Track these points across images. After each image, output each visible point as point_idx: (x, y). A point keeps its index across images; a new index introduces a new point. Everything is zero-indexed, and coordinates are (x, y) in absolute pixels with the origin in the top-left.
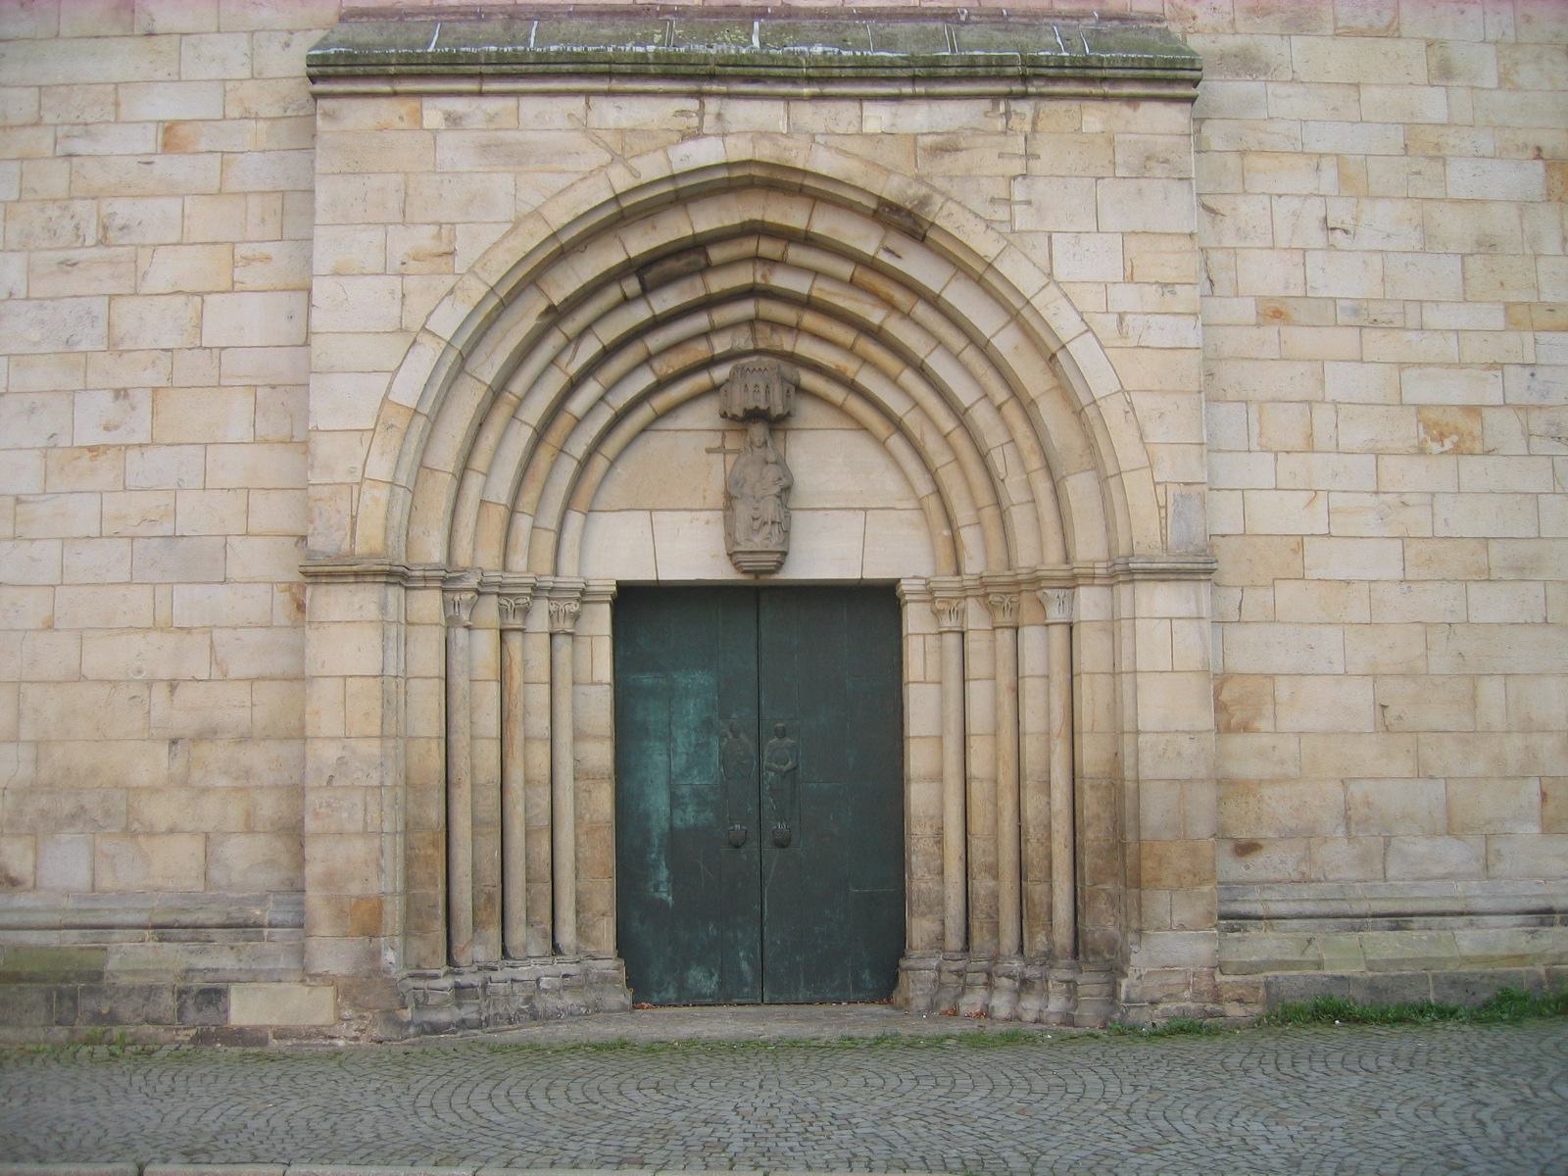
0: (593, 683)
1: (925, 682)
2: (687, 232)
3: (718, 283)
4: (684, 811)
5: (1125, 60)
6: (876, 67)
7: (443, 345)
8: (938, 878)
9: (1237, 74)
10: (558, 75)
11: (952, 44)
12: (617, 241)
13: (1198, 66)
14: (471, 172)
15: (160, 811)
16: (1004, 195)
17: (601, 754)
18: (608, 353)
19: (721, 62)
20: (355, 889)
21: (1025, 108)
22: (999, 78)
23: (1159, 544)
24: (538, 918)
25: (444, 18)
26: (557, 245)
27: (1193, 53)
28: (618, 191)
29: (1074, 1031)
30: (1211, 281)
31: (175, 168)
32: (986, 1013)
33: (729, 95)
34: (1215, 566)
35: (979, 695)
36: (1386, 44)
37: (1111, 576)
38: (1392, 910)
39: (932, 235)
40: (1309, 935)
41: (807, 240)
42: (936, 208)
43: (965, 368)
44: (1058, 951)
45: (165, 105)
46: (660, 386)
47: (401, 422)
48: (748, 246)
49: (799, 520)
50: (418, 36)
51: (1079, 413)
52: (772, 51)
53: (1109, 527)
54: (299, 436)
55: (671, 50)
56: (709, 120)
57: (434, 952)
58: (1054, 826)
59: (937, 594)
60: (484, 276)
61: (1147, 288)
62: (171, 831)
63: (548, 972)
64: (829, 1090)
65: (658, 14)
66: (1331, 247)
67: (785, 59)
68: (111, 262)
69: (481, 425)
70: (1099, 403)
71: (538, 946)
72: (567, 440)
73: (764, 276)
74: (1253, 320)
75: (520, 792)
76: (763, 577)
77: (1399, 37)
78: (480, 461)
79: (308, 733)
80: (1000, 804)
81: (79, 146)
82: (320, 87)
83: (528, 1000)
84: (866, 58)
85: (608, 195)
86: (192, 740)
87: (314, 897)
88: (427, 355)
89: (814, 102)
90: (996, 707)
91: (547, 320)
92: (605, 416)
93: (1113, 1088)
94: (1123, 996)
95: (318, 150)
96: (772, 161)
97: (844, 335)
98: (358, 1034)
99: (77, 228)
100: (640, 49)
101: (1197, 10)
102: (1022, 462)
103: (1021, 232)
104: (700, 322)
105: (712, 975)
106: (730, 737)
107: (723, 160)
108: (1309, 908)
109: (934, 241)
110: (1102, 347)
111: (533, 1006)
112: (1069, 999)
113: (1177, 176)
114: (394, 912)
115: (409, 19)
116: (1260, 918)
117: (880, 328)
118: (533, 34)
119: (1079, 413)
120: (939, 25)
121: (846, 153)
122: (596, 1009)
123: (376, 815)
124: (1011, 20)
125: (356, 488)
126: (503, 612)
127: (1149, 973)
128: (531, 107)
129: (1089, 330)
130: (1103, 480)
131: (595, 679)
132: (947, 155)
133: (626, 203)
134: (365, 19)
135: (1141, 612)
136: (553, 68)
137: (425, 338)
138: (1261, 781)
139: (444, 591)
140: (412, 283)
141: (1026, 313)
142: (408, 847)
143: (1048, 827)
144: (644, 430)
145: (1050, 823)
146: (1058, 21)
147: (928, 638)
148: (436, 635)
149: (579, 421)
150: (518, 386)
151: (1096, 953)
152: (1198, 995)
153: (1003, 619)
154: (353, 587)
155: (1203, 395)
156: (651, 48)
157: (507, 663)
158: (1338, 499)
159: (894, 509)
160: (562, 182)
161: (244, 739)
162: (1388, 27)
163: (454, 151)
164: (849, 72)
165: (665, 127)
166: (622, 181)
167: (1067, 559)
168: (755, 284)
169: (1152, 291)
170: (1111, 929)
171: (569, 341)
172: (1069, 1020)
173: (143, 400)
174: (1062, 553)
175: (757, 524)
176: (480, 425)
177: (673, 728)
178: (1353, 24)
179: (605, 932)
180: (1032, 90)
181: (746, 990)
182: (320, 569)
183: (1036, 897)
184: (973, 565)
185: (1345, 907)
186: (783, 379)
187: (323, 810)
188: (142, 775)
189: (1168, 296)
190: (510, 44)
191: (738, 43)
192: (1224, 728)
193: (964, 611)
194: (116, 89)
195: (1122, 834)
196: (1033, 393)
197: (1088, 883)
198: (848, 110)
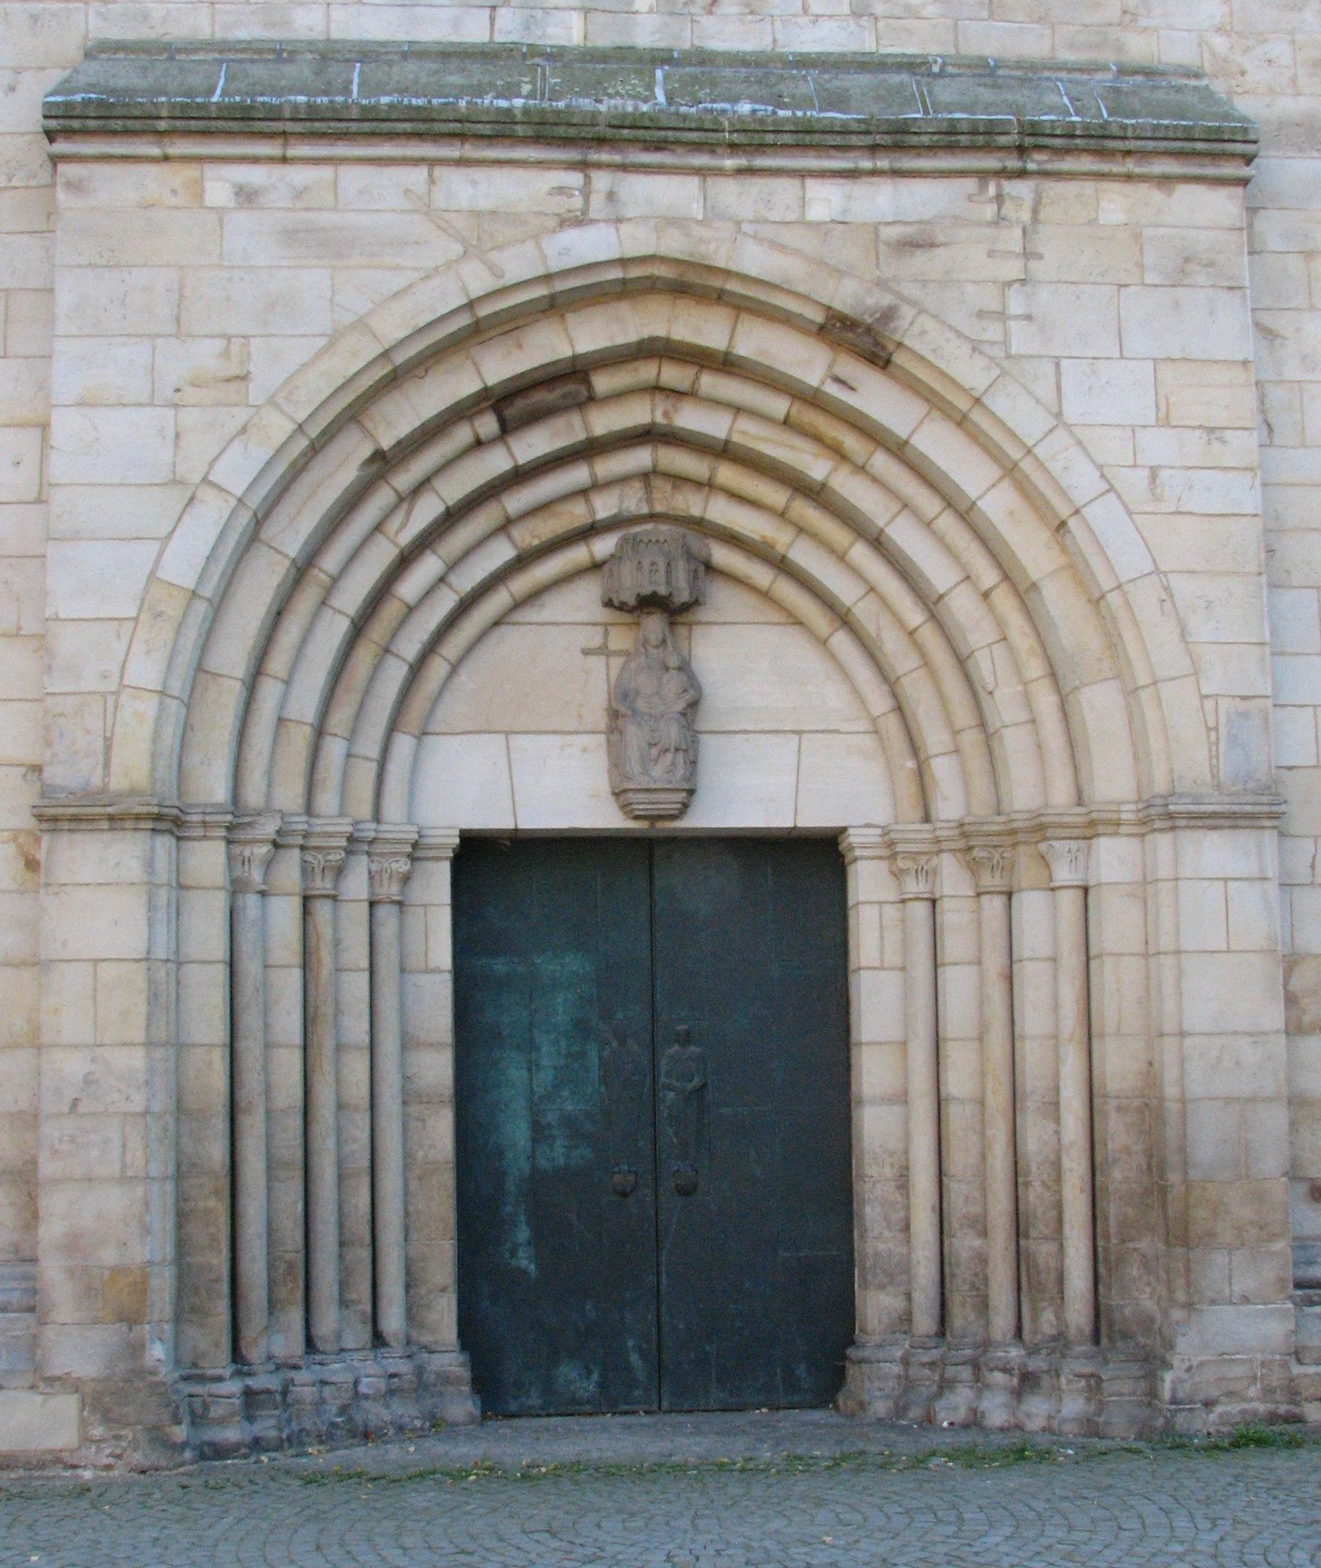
0: (428, 971)
1: (882, 968)
3: (604, 422)
4: (551, 1146)
5: (1156, 127)
6: (824, 132)
7: (233, 502)
8: (901, 1236)
9: (1300, 150)
10: (392, 136)
11: (924, 103)
12: (469, 362)
13: (1252, 137)
14: (270, 267)
16: (995, 306)
18: (452, 517)
19: (614, 122)
20: (109, 1256)
21: (1020, 189)
22: (988, 148)
23: (1208, 779)
24: (354, 1296)
25: (231, 56)
26: (389, 368)
27: (1244, 119)
28: (473, 296)
29: (1101, 1445)
30: (1269, 425)
32: (974, 1421)
33: (624, 168)
34: (1283, 808)
35: (958, 983)
37: (1143, 823)
39: (899, 358)
41: (726, 364)
42: (904, 324)
43: (941, 540)
44: (1072, 1333)
46: (523, 561)
47: (173, 609)
48: (647, 372)
49: (711, 747)
50: (195, 80)
51: (1097, 602)
52: (683, 109)
53: (1139, 754)
54: (30, 626)
55: (546, 105)
56: (597, 201)
57: (217, 1345)
58: (1067, 1164)
59: (900, 848)
61: (1187, 434)
64: (790, 1530)
65: (524, 56)
69: (279, 613)
70: (1126, 587)
71: (357, 1335)
72: (394, 634)
73: (666, 414)
75: (331, 1121)
76: (661, 825)
78: (278, 663)
79: (45, 1039)
80: (989, 1132)
82: (61, 147)
83: (343, 1410)
84: (809, 120)
85: (457, 301)
87: (53, 1271)
89: (741, 178)
90: (982, 1000)
91: (373, 469)
92: (445, 603)
93: (1181, 1521)
95: (59, 233)
96: (680, 256)
97: (775, 495)
98: (111, 1460)
100: (503, 103)
101: (1247, 66)
102: (1018, 668)
103: (1019, 357)
104: (578, 475)
105: (590, 1372)
106: (615, 1044)
107: (616, 255)
109: (902, 368)
110: (1130, 513)
111: (350, 1419)
112: (1088, 1400)
113: (1226, 284)
114: (163, 1287)
115: (183, 57)
117: (824, 485)
118: (356, 80)
119: (1097, 602)
120: (904, 77)
121: (782, 248)
122: (436, 1424)
123: (139, 1153)
124: (1000, 72)
125: (111, 700)
126: (306, 871)
127: (1202, 1364)
128: (353, 178)
129: (1111, 489)
130: (1131, 692)
131: (432, 965)
132: (918, 252)
133: (484, 311)
134: (121, 55)
135: (1187, 871)
136: (386, 126)
137: (206, 494)
139: (229, 842)
140: (190, 417)
141: (1027, 466)
143: (1057, 1166)
144: (497, 623)
145: (1059, 1158)
146: (1063, 75)
147: (887, 908)
148: (219, 902)
149: (411, 610)
150: (331, 561)
151: (1126, 1336)
152: (1268, 1392)
154: (107, 836)
155: (1264, 579)
156: (519, 102)
157: (312, 942)
159: (837, 731)
160: (399, 281)
164: (787, 139)
165: (536, 209)
166: (477, 281)
167: (1080, 800)
168: (653, 424)
169: (1194, 440)
170: (1149, 1305)
171: (401, 499)
172: (1091, 1428)
174: (1072, 791)
175: (654, 751)
176: (278, 615)
177: (535, 1031)
181: (638, 1392)
182: (60, 811)
183: (1041, 1261)
184: (949, 807)
186: (690, 556)
187: (65, 1147)
189: (1216, 445)
190: (325, 93)
191: (636, 97)
192: (1295, 1029)
193: (935, 871)
195: (1162, 1172)
196: (1035, 575)
197: (1114, 1241)
198: (785, 189)
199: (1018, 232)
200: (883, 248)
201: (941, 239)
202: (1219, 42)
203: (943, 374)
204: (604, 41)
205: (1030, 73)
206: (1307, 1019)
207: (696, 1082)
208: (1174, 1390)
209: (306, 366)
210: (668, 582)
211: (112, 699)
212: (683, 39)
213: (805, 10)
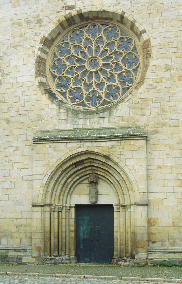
2: (80, 159)
3: (86, 165)
15: (15, 235)
16: (120, 154)
17: (73, 228)
18: (72, 175)
20: (38, 245)
21: (123, 141)
31: (17, 152)
36: (177, 128)
38: (173, 251)
40: (161, 254)
45: (16, 144)
46: (80, 178)
47: (44, 186)
48: (89, 160)
50: (46, 135)
55: (77, 136)
60: (54, 167)
62: (17, 238)
63: (64, 257)
65: (76, 130)
66: (168, 158)
67: (91, 137)
68: (9, 165)
71: (63, 254)
73: (92, 164)
74: (156, 168)
77: (179, 126)
78: (55, 190)
81: (6, 150)
86: (19, 226)
88: (47, 177)
92: (72, 182)
94: (134, 262)
97: (103, 171)
99: (6, 160)
100: (73, 136)
101: (149, 125)
104: (84, 170)
105: (88, 259)
107: (83, 151)
108: (162, 251)
110: (133, 174)
114: (42, 249)
116: (155, 252)
122: (70, 263)
126: (58, 209)
137: (46, 175)
138: (156, 233)
140: (45, 168)
142: (45, 240)
144: (79, 184)
150: (60, 180)
153: (124, 210)
158: (168, 194)
160: (63, 154)
161: (25, 226)
162: (177, 125)
163: (50, 151)
171: (66, 174)
173: (13, 182)
175: (92, 197)
178: (172, 125)
179: (73, 253)
180: (124, 139)
185: (167, 251)
186: (96, 177)
188: (13, 231)
194: (10, 142)
198: (100, 143)
199: (122, 146)
200: (109, 148)
201: (115, 147)
202: (146, 122)
203: (115, 161)
204: (84, 127)
205: (126, 128)
206: (152, 225)
207: (99, 230)
208: (135, 262)
209: (55, 163)
210: (93, 180)
211: (38, 194)
212: (92, 127)
213: (104, 122)
